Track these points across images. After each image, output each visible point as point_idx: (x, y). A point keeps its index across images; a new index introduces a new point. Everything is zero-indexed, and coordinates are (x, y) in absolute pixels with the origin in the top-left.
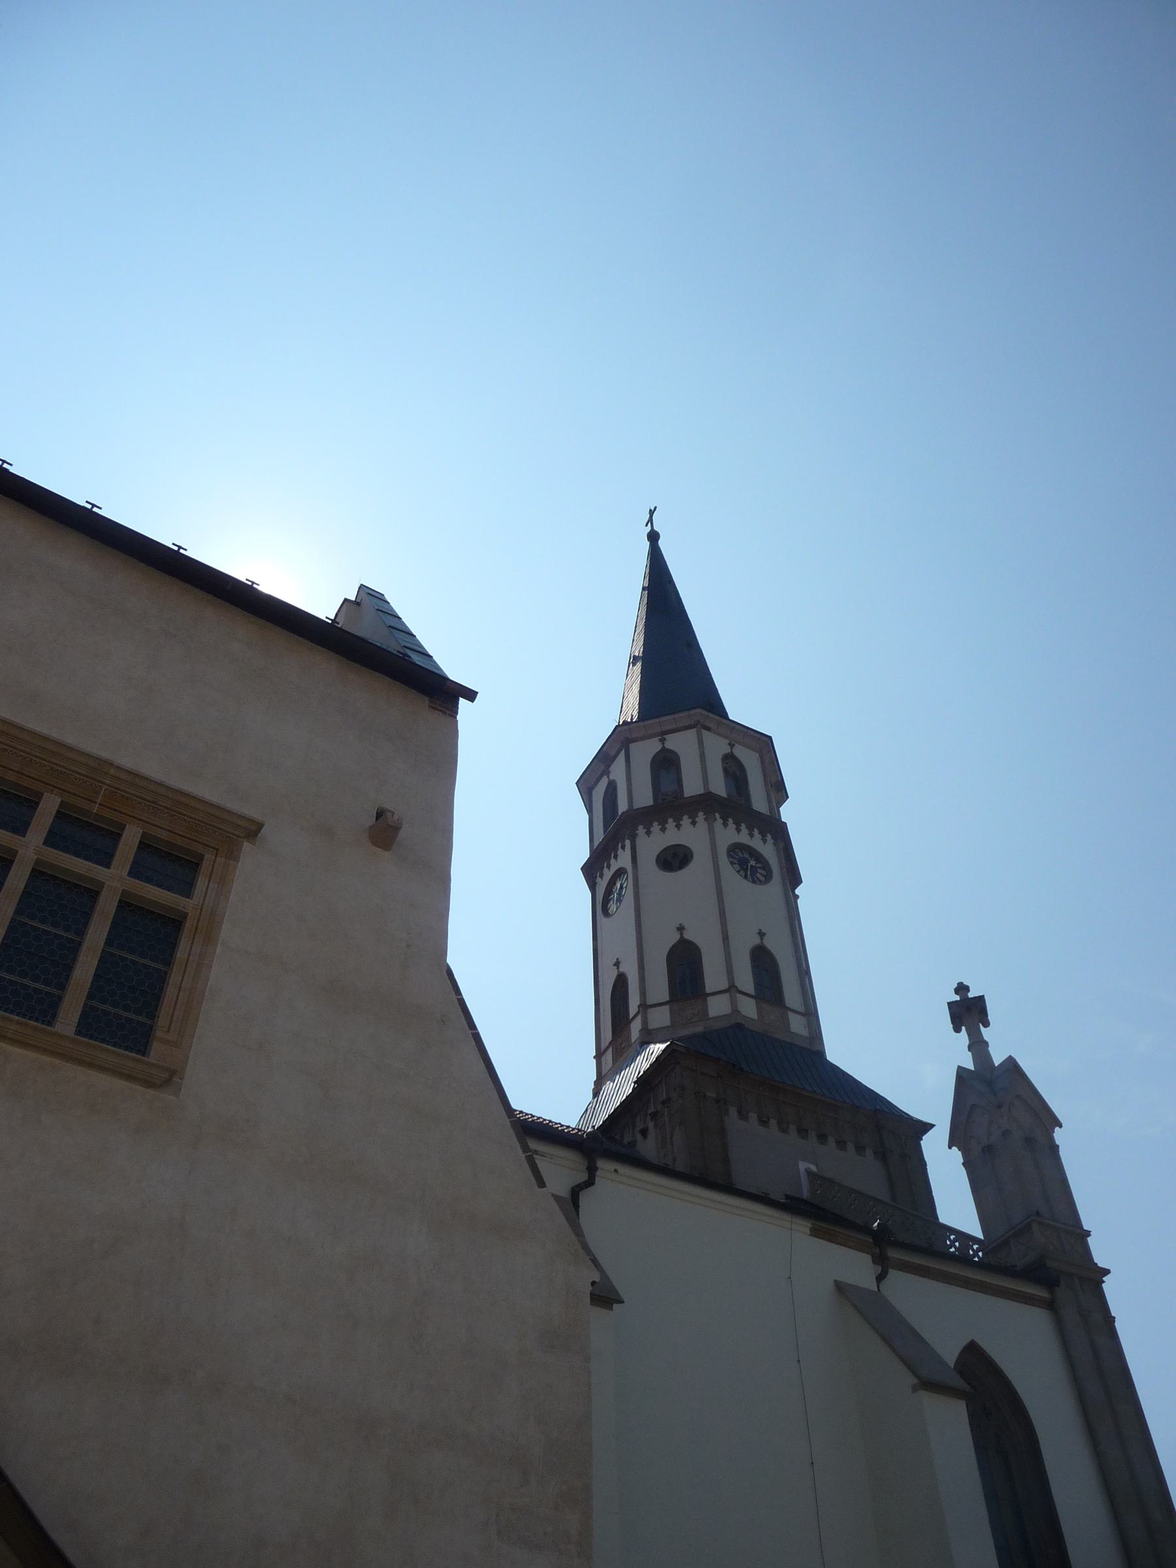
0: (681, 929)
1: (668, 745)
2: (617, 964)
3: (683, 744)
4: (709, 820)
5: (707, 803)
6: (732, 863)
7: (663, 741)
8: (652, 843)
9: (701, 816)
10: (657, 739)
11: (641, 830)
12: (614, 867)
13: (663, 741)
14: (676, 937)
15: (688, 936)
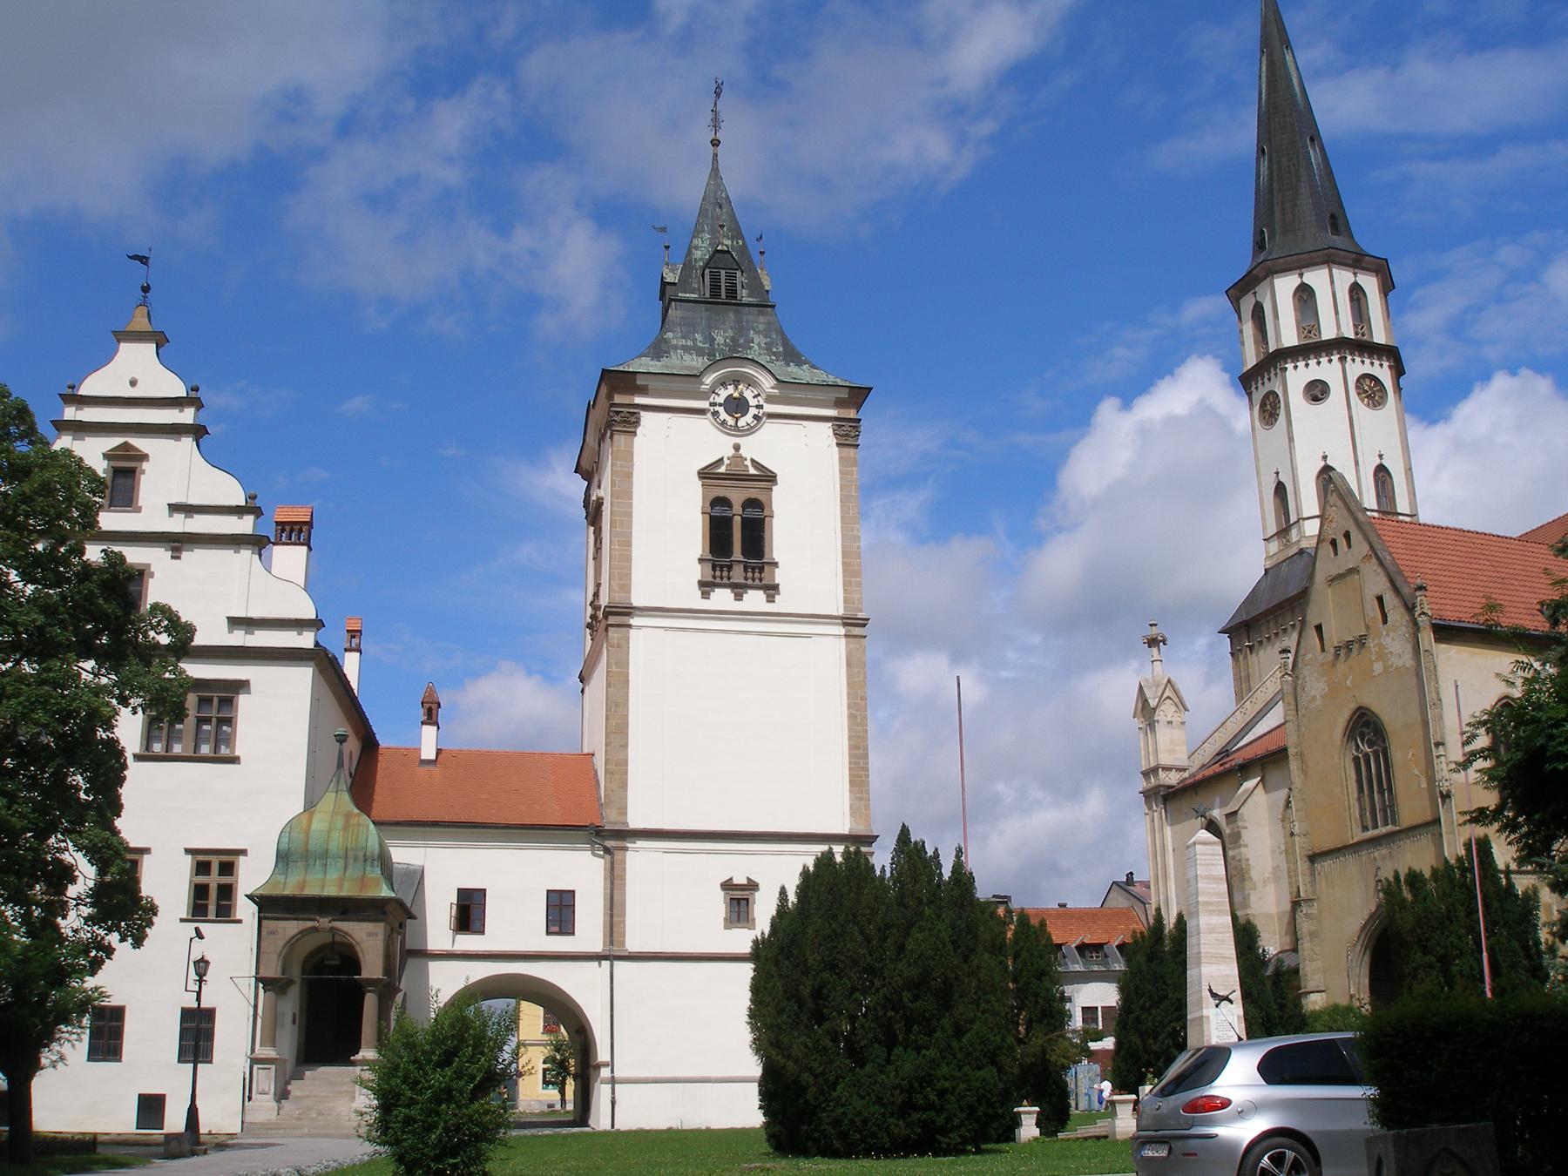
0: (1325, 458)
1: (1306, 282)
2: (1277, 473)
3: (1317, 278)
4: (1342, 360)
5: (1340, 346)
6: (1359, 394)
7: (1301, 275)
8: (1297, 376)
9: (1335, 358)
10: (1298, 271)
11: (1290, 366)
12: (1268, 387)
13: (1301, 275)
14: (1323, 464)
15: (1329, 462)
